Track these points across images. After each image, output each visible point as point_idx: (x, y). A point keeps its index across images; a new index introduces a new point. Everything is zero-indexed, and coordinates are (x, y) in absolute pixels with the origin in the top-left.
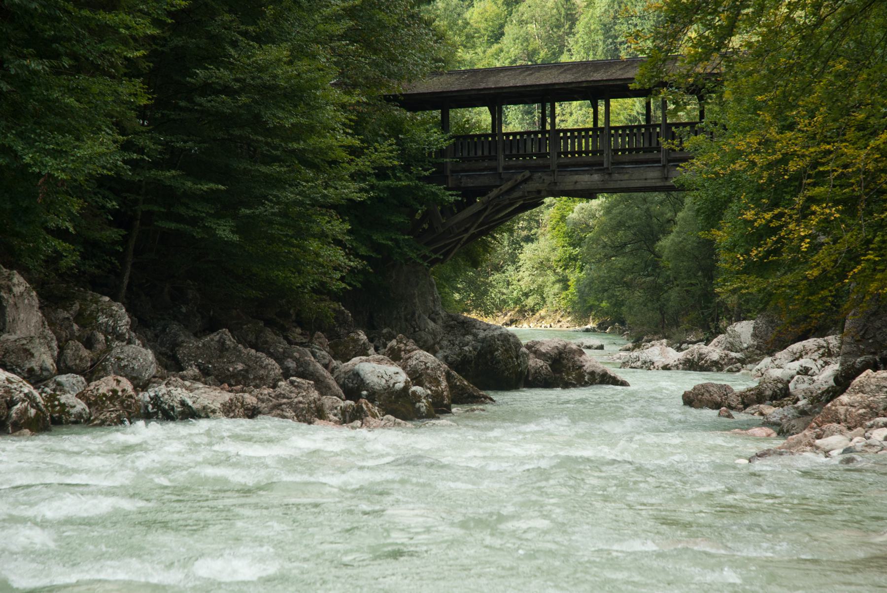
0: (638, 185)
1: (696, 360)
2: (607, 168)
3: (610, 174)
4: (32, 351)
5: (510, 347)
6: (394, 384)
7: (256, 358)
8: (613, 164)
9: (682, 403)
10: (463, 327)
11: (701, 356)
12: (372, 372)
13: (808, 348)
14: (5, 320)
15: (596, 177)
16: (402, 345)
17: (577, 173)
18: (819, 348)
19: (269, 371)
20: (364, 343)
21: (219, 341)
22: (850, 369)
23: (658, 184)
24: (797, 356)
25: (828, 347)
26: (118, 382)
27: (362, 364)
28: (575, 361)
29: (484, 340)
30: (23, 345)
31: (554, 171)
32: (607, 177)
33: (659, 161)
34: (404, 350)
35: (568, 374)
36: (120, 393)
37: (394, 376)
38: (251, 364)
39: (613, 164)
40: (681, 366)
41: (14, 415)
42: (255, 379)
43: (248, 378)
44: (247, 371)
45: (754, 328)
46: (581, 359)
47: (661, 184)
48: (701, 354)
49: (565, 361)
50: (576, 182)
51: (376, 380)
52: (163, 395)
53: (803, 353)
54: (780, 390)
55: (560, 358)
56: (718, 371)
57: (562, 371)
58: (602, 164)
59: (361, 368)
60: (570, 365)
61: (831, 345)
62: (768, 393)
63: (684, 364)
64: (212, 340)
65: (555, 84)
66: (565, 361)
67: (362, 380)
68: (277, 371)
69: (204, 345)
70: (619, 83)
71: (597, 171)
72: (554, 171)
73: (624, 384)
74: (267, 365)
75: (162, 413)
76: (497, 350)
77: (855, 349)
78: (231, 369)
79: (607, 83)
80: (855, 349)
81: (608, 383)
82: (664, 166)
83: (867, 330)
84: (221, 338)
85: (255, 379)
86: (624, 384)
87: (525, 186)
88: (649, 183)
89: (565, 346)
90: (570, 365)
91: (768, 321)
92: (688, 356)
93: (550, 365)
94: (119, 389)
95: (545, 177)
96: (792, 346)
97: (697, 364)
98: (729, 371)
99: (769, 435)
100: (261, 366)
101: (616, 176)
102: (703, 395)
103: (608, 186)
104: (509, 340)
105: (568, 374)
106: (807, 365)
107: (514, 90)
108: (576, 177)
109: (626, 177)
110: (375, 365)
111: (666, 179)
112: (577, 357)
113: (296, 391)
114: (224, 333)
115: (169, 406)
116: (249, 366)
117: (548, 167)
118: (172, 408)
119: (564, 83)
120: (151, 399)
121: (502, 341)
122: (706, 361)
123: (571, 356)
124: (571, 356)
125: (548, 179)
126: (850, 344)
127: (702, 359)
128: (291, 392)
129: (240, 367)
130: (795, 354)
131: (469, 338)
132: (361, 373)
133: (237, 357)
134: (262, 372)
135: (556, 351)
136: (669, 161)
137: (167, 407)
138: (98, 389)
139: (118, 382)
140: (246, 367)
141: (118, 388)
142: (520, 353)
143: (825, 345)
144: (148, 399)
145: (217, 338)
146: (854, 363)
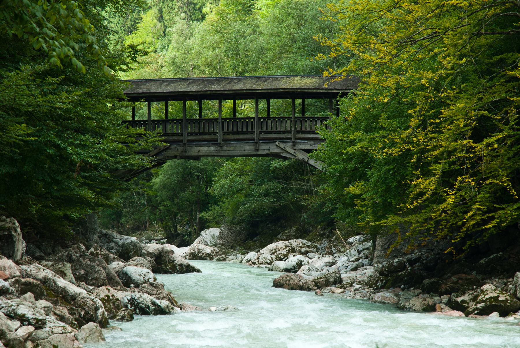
0: (240, 154)
1: (196, 253)
2: (220, 143)
3: (221, 147)
4: (66, 272)
5: (137, 250)
6: (148, 279)
7: (91, 266)
8: (223, 140)
9: (272, 284)
10: (106, 238)
11: (199, 251)
12: (135, 272)
13: (280, 247)
14: (14, 250)
15: (212, 148)
16: (98, 251)
17: (199, 145)
18: (286, 247)
19: (100, 275)
20: (84, 251)
21: (67, 256)
22: (391, 267)
23: (252, 154)
24: (273, 251)
25: (291, 247)
26: (109, 290)
27: (128, 267)
28: (169, 258)
29: (123, 245)
30: (60, 268)
31: (185, 144)
32: (219, 148)
33: (253, 139)
34: (101, 254)
35: (166, 266)
36: (111, 298)
37: (147, 274)
38: (89, 270)
39: (223, 140)
40: (188, 257)
41: (100, 316)
42: (92, 280)
43: (88, 279)
44: (86, 275)
45: (220, 233)
46: (173, 256)
47: (255, 153)
48: (199, 250)
49: (164, 258)
50: (199, 151)
51: (138, 277)
52: (138, 298)
53: (277, 250)
54: (338, 278)
55: (160, 255)
56: (210, 260)
57: (162, 264)
58: (217, 141)
59: (128, 270)
60: (167, 260)
61: (293, 246)
62: (332, 280)
63: (190, 256)
64: (63, 255)
65: (189, 92)
66: (164, 258)
67: (130, 277)
68: (104, 274)
69: (59, 258)
70: (231, 92)
71: (213, 145)
72: (185, 144)
73: (199, 271)
74: (98, 270)
75: (139, 310)
76: (131, 252)
77: (384, 254)
78: (77, 274)
79: (223, 92)
80: (384, 254)
81: (190, 272)
82: (257, 143)
83: (391, 243)
84: (68, 254)
85: (92, 280)
86: (199, 271)
87: (166, 153)
88: (246, 153)
89: (163, 249)
90: (167, 260)
91: (228, 229)
92: (192, 251)
93: (155, 260)
94: (110, 295)
95: (179, 148)
96: (269, 246)
97: (197, 255)
98: (218, 260)
99: (461, 316)
100: (95, 271)
101: (225, 148)
102: (289, 281)
103: (220, 154)
104: (136, 246)
105: (166, 266)
106: (301, 259)
107: (162, 94)
108: (199, 148)
109: (232, 148)
110: (134, 267)
111: (258, 150)
112: (170, 255)
113: (156, 290)
114: (70, 250)
115: (146, 305)
116: (88, 272)
117: (182, 141)
118: (148, 307)
119: (195, 91)
120: (129, 301)
121: (133, 246)
122: (203, 254)
123: (167, 254)
124: (167, 254)
125: (181, 149)
126: (381, 251)
127: (200, 253)
128: (153, 290)
129: (82, 272)
130: (272, 250)
131: (112, 244)
132: (128, 273)
133: (80, 265)
134: (96, 275)
135: (158, 252)
136: (260, 140)
137: (144, 306)
138: (99, 295)
139: (109, 290)
140: (86, 272)
141: (109, 294)
142: (142, 253)
143: (290, 245)
144: (127, 301)
145: (66, 254)
146: (393, 263)
